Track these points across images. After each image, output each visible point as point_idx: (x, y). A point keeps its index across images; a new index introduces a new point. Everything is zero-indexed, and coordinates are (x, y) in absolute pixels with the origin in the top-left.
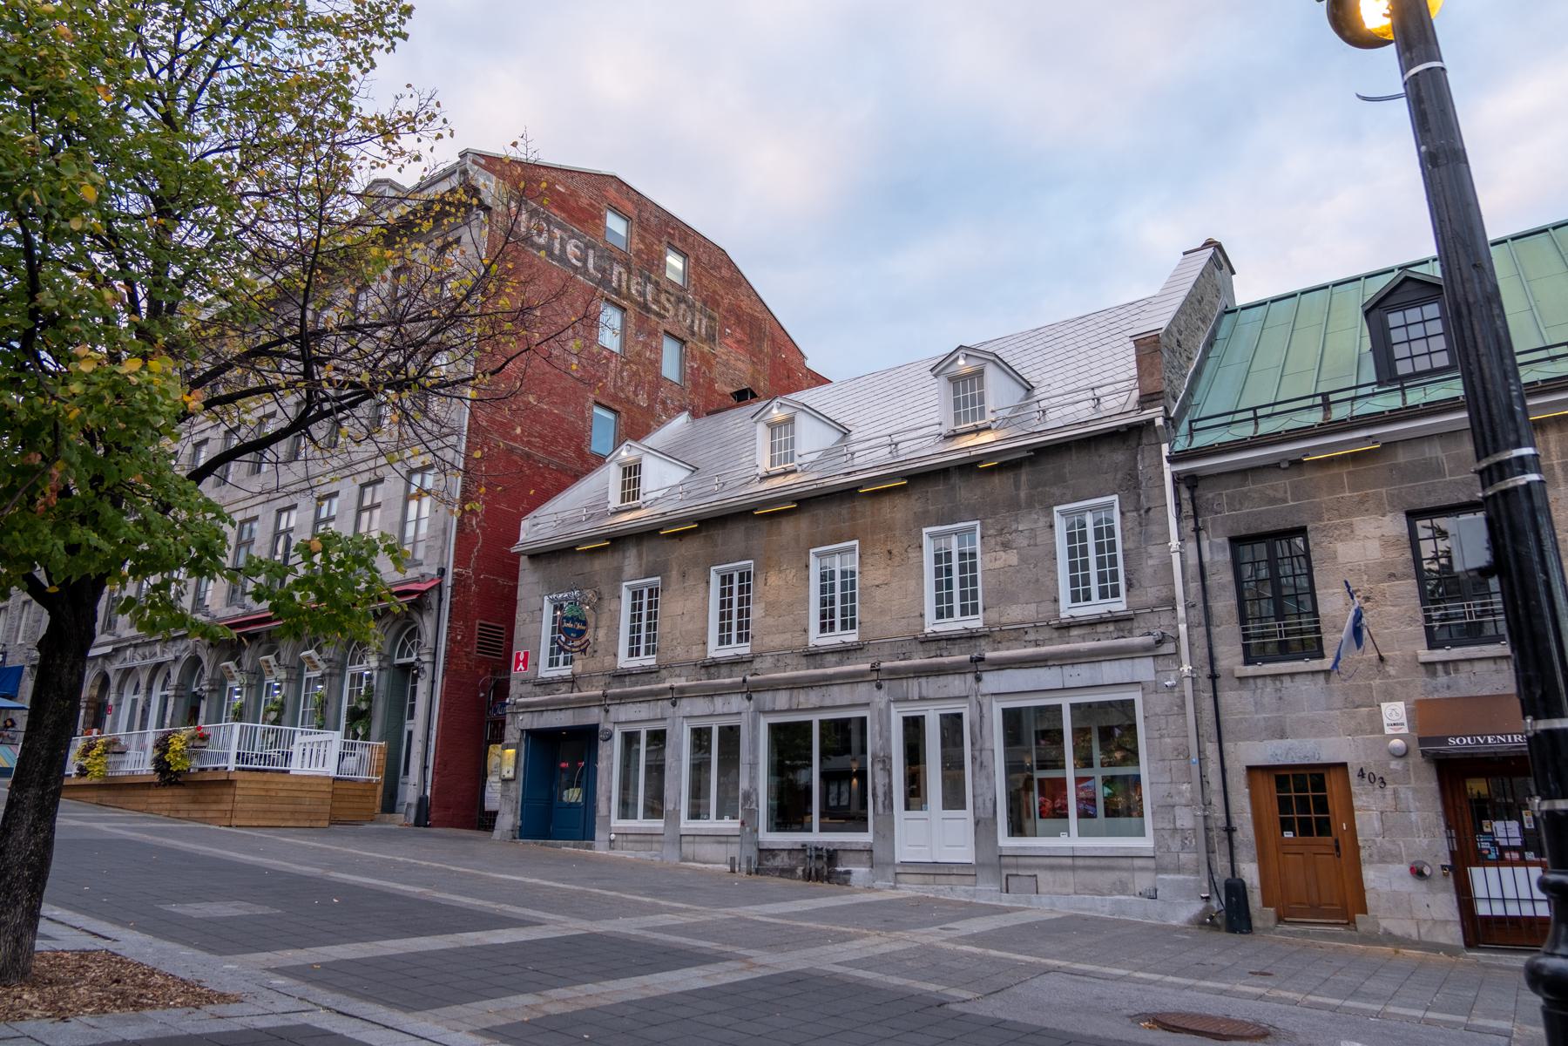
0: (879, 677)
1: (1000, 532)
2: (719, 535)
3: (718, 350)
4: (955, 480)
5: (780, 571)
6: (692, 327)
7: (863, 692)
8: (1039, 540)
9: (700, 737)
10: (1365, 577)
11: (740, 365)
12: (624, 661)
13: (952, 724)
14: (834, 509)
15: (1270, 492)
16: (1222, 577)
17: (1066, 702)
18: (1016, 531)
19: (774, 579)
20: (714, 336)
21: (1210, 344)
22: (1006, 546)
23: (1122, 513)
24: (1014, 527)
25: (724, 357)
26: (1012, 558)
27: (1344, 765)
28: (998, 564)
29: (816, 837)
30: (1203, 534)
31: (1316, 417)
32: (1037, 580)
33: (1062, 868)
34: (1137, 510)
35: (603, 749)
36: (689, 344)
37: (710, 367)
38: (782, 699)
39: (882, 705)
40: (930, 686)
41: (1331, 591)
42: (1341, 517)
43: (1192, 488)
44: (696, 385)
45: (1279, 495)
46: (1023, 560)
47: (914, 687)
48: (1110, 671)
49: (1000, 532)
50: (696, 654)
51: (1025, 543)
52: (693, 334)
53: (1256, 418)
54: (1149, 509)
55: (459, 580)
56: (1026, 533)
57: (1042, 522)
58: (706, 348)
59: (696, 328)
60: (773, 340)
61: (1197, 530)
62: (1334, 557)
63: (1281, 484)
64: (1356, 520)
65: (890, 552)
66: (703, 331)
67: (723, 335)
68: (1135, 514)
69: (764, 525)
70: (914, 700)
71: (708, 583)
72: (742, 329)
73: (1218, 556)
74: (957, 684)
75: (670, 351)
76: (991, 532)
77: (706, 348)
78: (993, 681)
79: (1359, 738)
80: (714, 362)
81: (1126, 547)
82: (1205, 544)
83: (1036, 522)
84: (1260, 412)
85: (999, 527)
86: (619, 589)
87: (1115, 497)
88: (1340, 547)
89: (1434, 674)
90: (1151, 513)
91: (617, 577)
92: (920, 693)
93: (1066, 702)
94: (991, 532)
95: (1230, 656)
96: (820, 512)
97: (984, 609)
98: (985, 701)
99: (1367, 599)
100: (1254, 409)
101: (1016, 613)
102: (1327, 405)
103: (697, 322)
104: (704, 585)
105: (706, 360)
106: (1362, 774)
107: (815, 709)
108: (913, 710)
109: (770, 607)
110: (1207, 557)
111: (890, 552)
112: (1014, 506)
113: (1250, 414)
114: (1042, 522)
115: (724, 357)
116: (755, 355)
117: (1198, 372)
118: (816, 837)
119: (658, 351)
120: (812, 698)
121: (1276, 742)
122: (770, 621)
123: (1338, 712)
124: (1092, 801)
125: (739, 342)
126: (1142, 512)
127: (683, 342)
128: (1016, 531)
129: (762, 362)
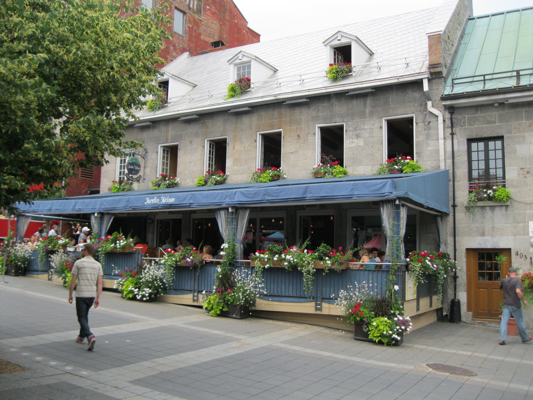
1: (355, 129)
2: (209, 122)
3: (202, 18)
4: (334, 101)
5: (242, 143)
6: (189, 5)
8: (374, 134)
10: (528, 162)
11: (213, 26)
14: (270, 112)
15: (488, 118)
18: (363, 129)
19: (238, 147)
20: (201, 10)
21: (462, 37)
22: (358, 136)
24: (362, 127)
25: (206, 22)
27: (509, 250)
28: (354, 145)
30: (455, 136)
31: (512, 83)
32: (372, 154)
36: (188, 14)
37: (198, 27)
41: (512, 168)
42: (520, 132)
43: (452, 113)
44: (191, 36)
45: (493, 119)
49: (355, 129)
51: (367, 135)
52: (190, 9)
53: (484, 80)
54: (430, 122)
58: (196, 16)
59: (191, 6)
60: (231, 12)
61: (452, 134)
62: (515, 151)
63: (494, 114)
64: (526, 134)
65: (299, 136)
66: (195, 7)
67: (205, 10)
68: (423, 124)
69: (233, 119)
71: (204, 147)
72: (215, 6)
75: (178, 17)
76: (351, 129)
77: (196, 16)
79: (518, 237)
80: (200, 25)
82: (455, 141)
83: (373, 125)
84: (487, 77)
85: (355, 126)
88: (518, 147)
90: (431, 124)
94: (351, 129)
96: (263, 113)
99: (528, 172)
100: (484, 76)
102: (518, 76)
103: (192, 2)
104: (201, 147)
105: (196, 23)
106: (517, 254)
109: (236, 161)
110: (456, 148)
111: (299, 136)
112: (362, 115)
113: (482, 78)
114: (377, 125)
115: (206, 22)
116: (222, 21)
117: (456, 52)
119: (172, 17)
122: (236, 168)
123: (509, 225)
125: (213, 14)
126: (426, 123)
127: (184, 13)
128: (363, 129)
129: (224, 24)
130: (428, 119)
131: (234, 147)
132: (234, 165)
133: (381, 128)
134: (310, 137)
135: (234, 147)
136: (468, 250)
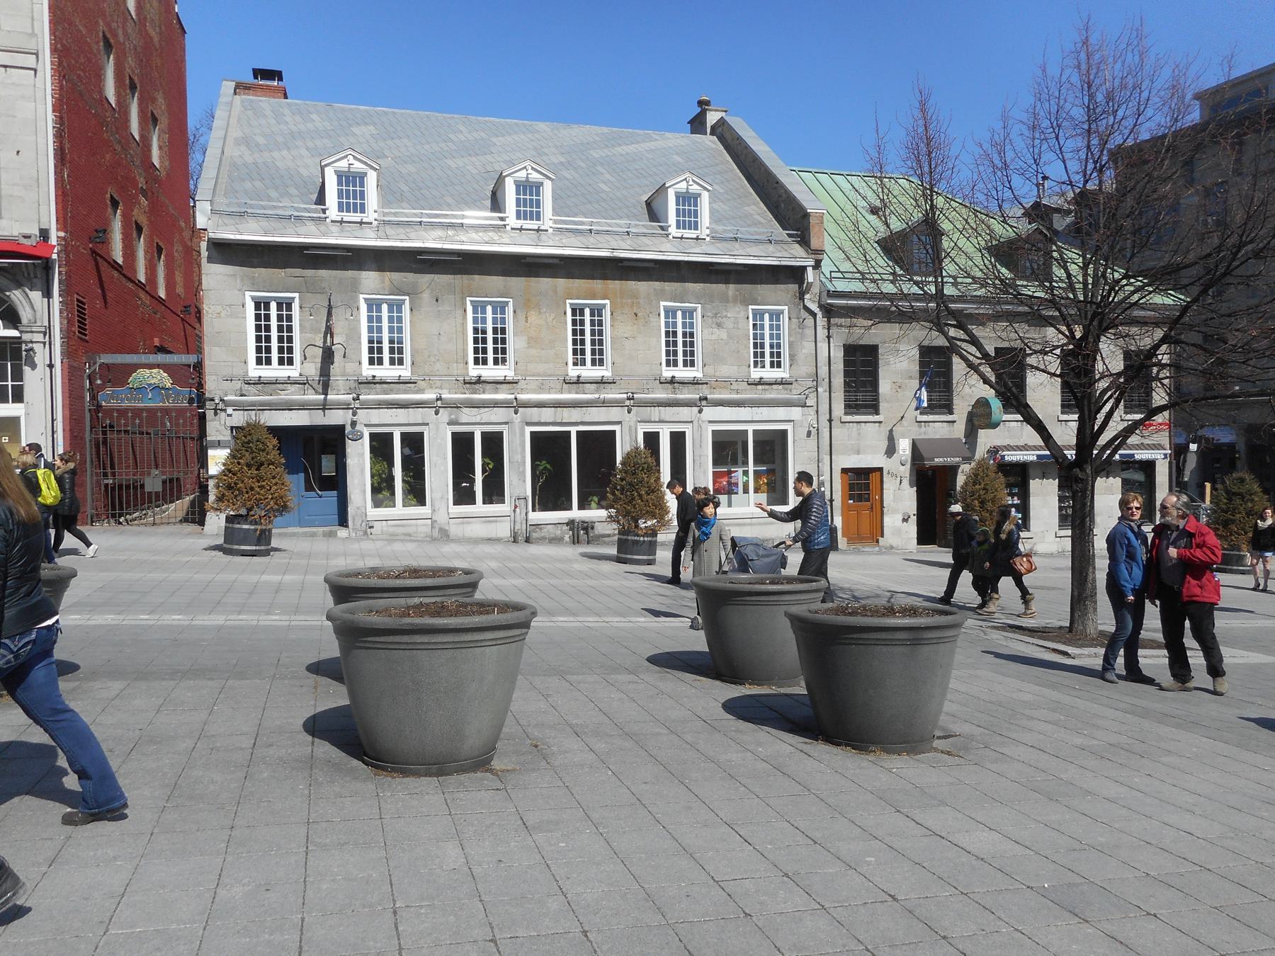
0: (632, 403)
5: (540, 313)
7: (615, 413)
8: (740, 326)
9: (462, 444)
12: (368, 371)
13: (678, 440)
16: (839, 366)
17: (750, 428)
18: (726, 316)
22: (719, 325)
23: (790, 319)
24: (725, 314)
26: (723, 334)
28: (714, 337)
29: (575, 513)
32: (738, 352)
33: (744, 525)
34: (798, 318)
35: (351, 447)
38: (547, 415)
39: (632, 424)
40: (667, 413)
46: (730, 337)
47: (656, 413)
48: (781, 413)
50: (456, 369)
51: (731, 326)
55: (66, 247)
56: (732, 319)
57: (742, 314)
61: (829, 337)
70: (655, 422)
73: (838, 355)
74: (685, 413)
78: (710, 413)
81: (792, 339)
85: (714, 312)
86: (357, 300)
87: (786, 307)
89: (920, 427)
91: (355, 288)
92: (660, 417)
93: (750, 428)
94: (709, 314)
95: (839, 408)
97: (704, 365)
98: (703, 425)
101: (726, 370)
104: (460, 312)
107: (574, 424)
108: (651, 428)
112: (725, 299)
114: (742, 314)
118: (575, 513)
120: (575, 415)
121: (856, 456)
122: (533, 352)
124: (736, 485)
128: (726, 316)
130: (804, 314)
131: (527, 318)
132: (528, 347)
133: (748, 318)
134: (653, 319)
135: (527, 318)
136: (843, 469)
